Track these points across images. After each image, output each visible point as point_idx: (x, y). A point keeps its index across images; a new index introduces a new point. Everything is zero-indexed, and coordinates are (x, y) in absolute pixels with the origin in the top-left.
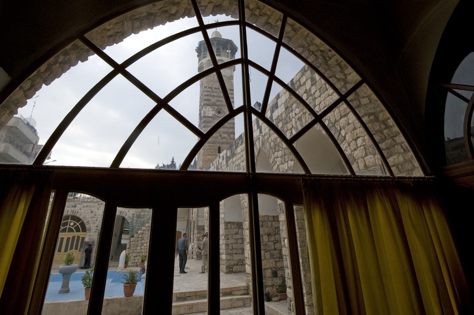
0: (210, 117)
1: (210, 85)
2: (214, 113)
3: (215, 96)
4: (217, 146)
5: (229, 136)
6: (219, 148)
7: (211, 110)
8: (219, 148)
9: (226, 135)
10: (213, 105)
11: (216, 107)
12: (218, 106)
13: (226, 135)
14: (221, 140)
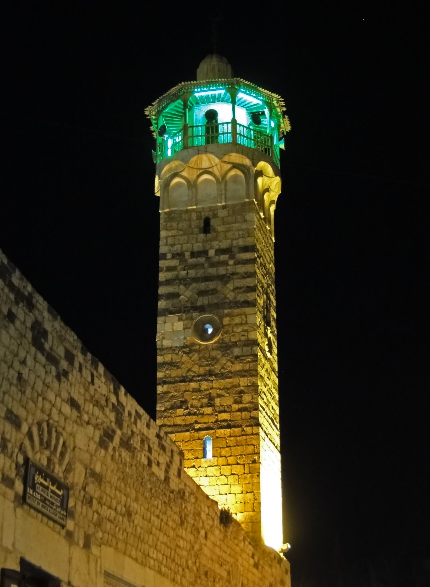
3: (195, 280)
13: (228, 401)
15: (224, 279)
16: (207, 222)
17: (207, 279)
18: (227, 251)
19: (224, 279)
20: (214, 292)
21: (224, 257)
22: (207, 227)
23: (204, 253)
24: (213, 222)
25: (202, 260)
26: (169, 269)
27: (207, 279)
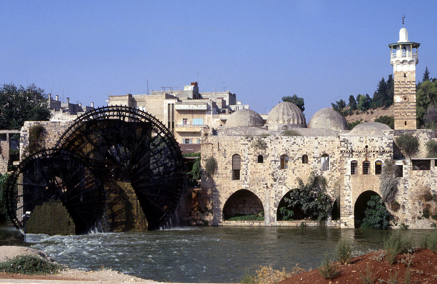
0: (400, 103)
1: (398, 80)
2: (401, 99)
3: (402, 88)
5: (412, 114)
6: (406, 122)
7: (400, 97)
8: (406, 122)
9: (410, 114)
10: (401, 94)
11: (403, 96)
12: (404, 94)
15: (409, 88)
16: (405, 74)
17: (405, 88)
19: (409, 88)
20: (407, 91)
21: (409, 83)
22: (405, 76)
23: (405, 82)
26: (397, 85)
27: (405, 88)
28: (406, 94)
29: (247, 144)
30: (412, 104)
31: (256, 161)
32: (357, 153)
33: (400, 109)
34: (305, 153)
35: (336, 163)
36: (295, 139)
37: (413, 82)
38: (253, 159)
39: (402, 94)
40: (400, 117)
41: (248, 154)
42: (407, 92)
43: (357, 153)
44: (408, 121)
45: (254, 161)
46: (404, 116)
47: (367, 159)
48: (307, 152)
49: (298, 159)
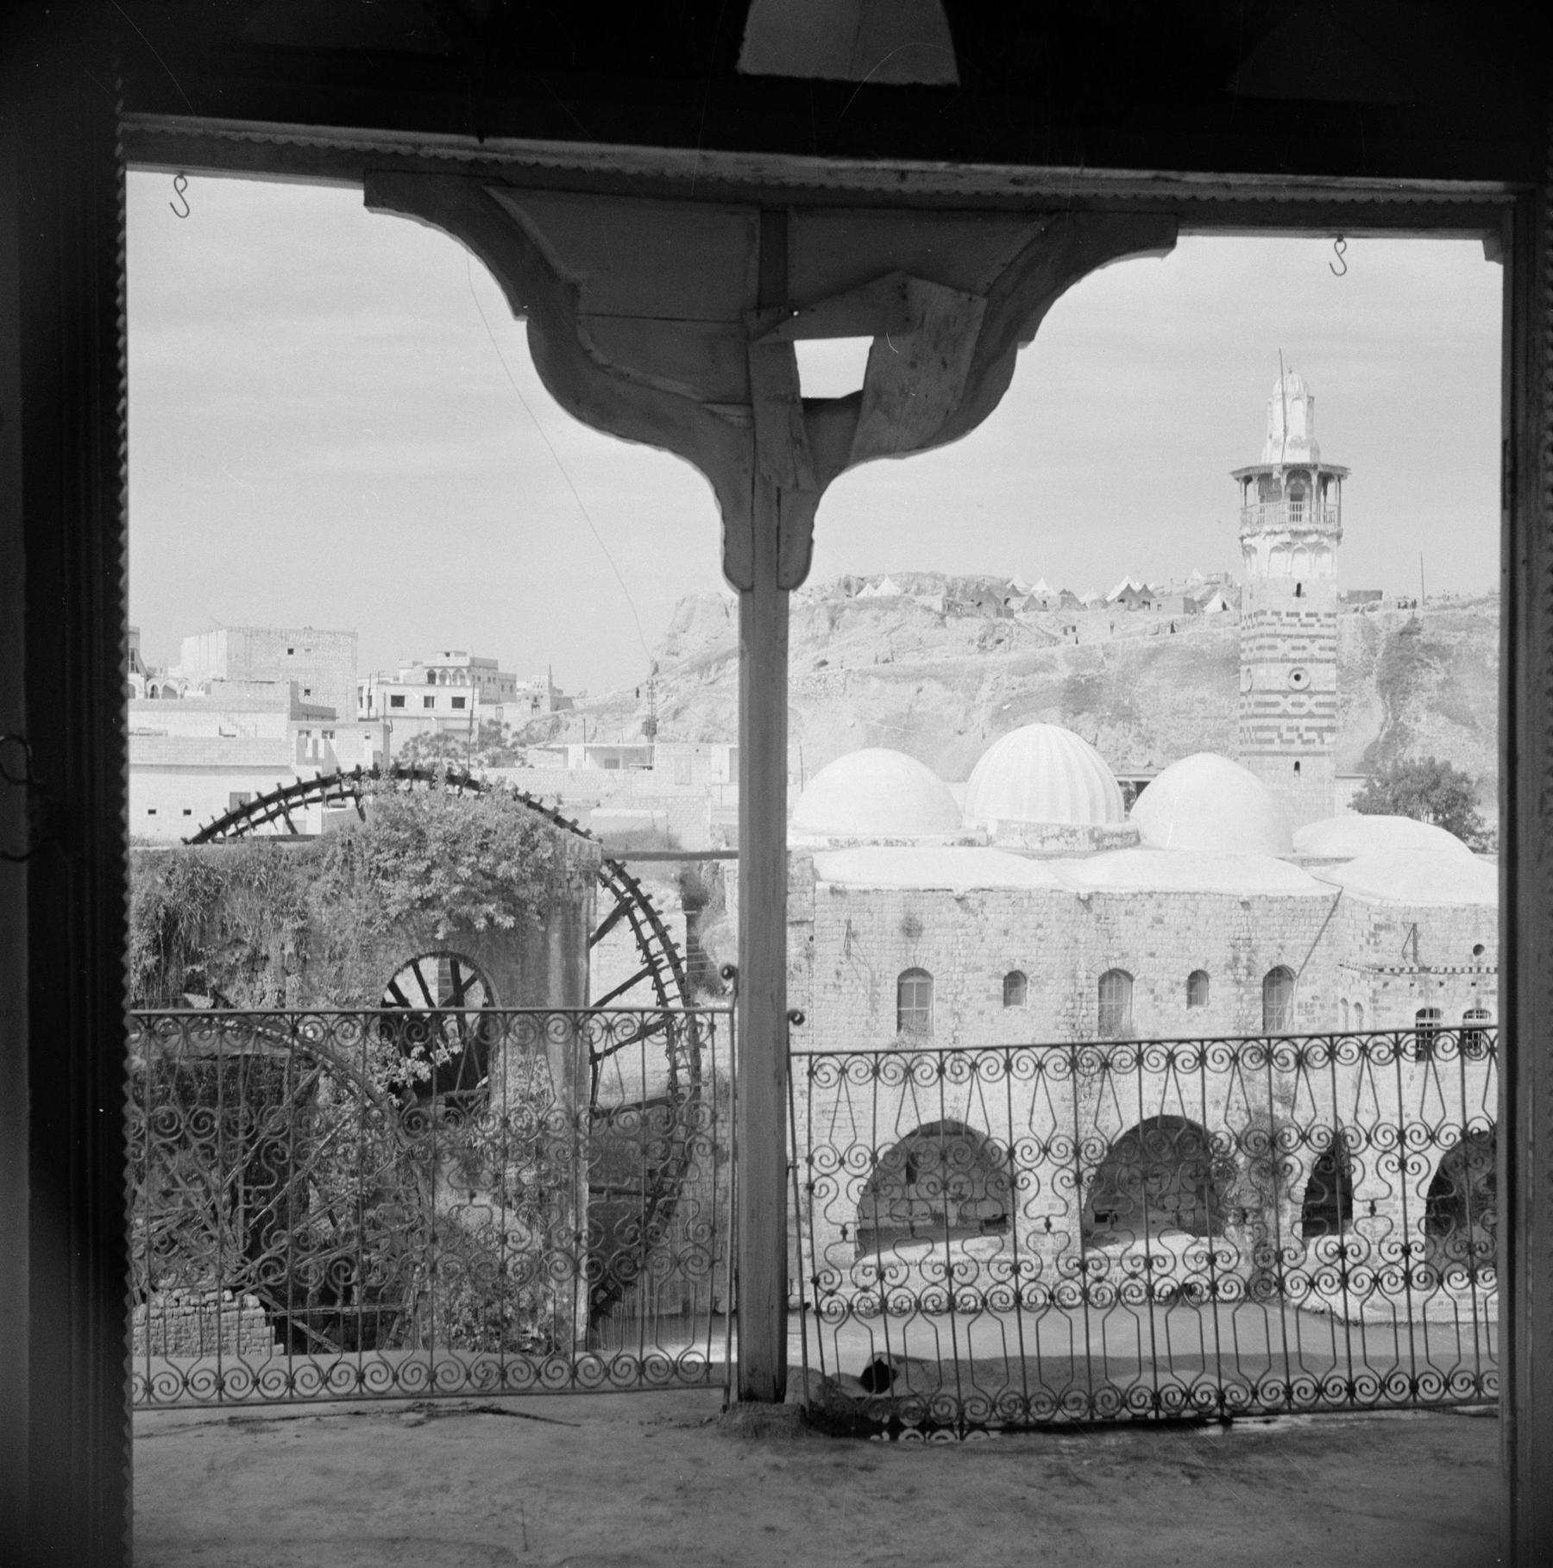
3: (1290, 636)
4: (1293, 761)
8: (1297, 766)
9: (1313, 735)
11: (1290, 666)
12: (1294, 661)
14: (1302, 748)
15: (1313, 638)
16: (1299, 586)
18: (1316, 615)
19: (1313, 638)
21: (1313, 620)
22: (1298, 593)
23: (1297, 614)
24: (1303, 589)
25: (1295, 620)
28: (1301, 660)
29: (962, 926)
30: (1320, 698)
31: (997, 997)
32: (1442, 978)
33: (1280, 716)
34: (1200, 966)
35: (1322, 1006)
36: (1160, 906)
37: (1329, 615)
38: (987, 990)
39: (1285, 660)
40: (1276, 747)
41: (966, 968)
42: (1305, 655)
43: (1442, 978)
44: (1304, 762)
45: (989, 998)
46: (1291, 742)
47: (1478, 1002)
48: (1207, 962)
49: (1172, 991)
